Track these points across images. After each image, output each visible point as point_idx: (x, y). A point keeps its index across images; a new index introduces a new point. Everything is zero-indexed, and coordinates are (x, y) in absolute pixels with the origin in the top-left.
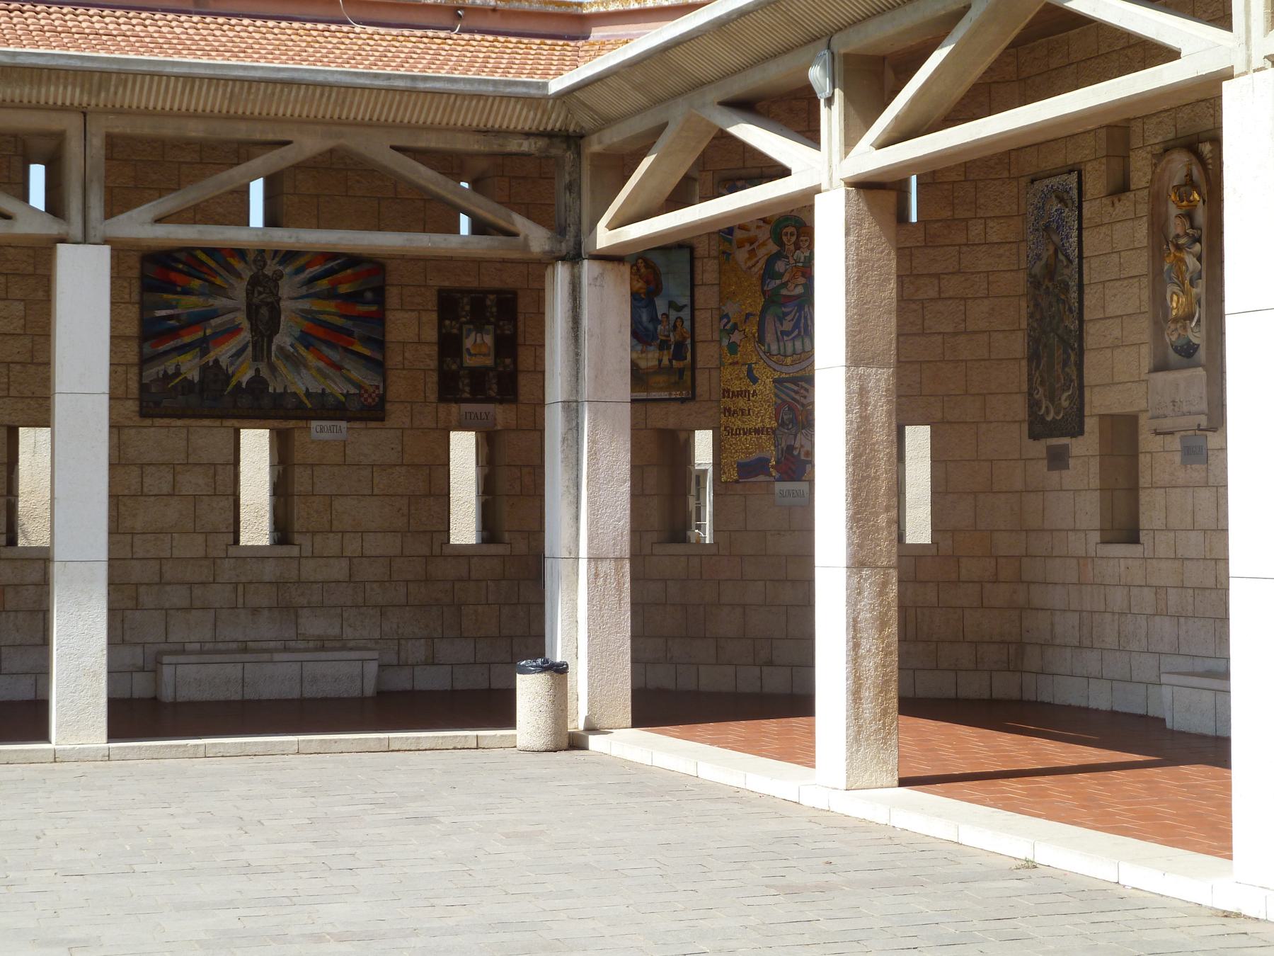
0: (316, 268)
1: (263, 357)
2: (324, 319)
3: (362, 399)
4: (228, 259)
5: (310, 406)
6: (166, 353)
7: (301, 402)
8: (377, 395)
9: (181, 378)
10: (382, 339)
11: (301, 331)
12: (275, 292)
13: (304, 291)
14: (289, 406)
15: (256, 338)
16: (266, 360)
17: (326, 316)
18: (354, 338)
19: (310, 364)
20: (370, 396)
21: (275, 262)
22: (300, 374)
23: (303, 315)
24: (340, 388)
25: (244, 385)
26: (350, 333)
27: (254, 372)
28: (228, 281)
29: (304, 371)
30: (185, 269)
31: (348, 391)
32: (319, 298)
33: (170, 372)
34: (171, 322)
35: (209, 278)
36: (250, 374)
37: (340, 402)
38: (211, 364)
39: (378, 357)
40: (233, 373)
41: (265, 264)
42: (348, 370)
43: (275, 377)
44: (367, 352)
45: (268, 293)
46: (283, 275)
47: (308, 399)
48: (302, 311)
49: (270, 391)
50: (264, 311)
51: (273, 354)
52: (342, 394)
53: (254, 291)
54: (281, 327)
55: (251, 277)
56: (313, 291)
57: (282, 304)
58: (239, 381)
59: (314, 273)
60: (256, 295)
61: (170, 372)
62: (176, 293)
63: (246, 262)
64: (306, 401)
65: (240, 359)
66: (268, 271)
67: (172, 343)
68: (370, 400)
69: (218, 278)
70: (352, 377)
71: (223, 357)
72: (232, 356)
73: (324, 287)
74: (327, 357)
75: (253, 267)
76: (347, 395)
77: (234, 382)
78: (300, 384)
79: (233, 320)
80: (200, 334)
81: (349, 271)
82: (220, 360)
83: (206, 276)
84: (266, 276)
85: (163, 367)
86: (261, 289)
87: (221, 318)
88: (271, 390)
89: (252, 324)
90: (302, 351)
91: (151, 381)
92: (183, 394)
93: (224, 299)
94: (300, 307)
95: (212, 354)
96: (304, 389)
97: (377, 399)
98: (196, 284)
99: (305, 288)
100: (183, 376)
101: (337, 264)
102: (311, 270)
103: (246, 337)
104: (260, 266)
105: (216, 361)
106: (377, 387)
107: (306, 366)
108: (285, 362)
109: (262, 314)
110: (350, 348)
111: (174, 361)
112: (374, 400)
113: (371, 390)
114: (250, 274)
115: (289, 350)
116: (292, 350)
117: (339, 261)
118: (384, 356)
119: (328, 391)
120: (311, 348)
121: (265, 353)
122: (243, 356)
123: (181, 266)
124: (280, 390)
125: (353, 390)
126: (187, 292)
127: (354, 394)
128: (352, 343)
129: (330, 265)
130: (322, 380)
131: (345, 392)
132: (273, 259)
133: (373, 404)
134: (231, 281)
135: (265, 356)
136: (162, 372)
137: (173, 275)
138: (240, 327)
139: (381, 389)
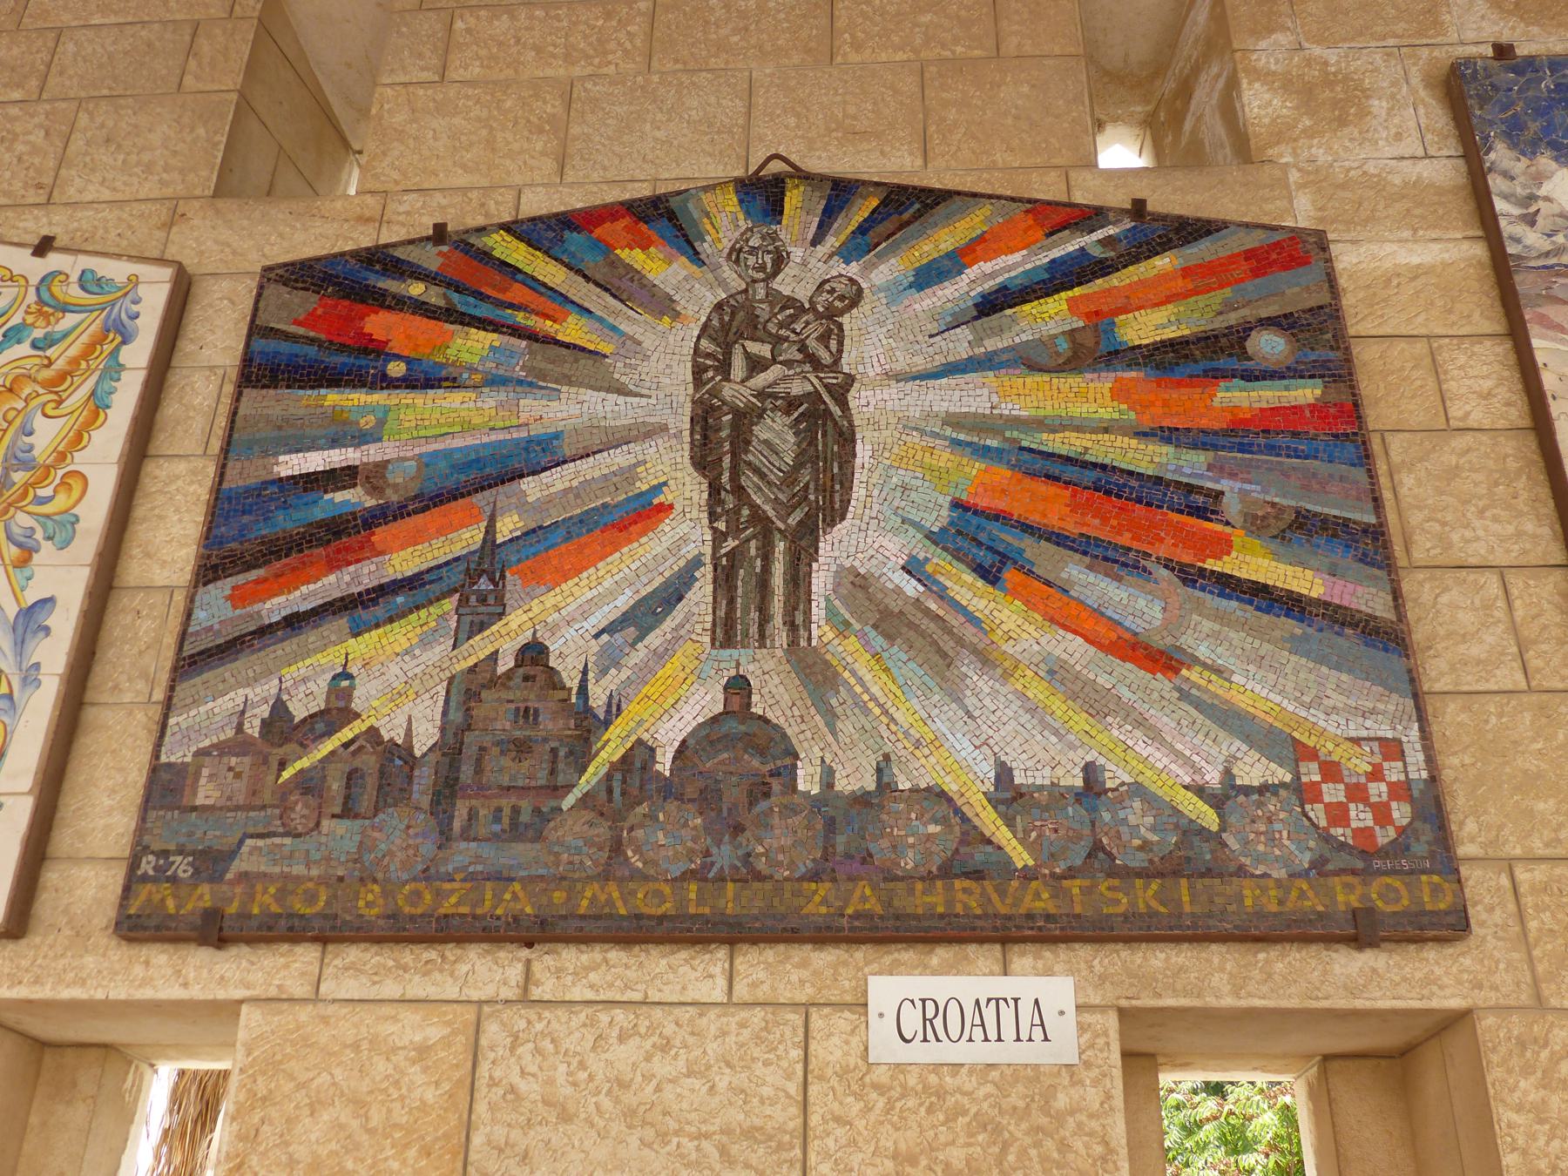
0: (1017, 257)
1: (765, 619)
2: (1063, 450)
3: (1317, 813)
4: (623, 254)
5: (1021, 857)
6: (294, 622)
7: (974, 836)
8: (1400, 791)
9: (346, 734)
10: (1373, 520)
11: (957, 504)
12: (826, 358)
13: (961, 344)
14: (909, 862)
15: (731, 543)
16: (781, 638)
17: (1072, 436)
18: (1228, 523)
19: (1007, 647)
20: (1357, 793)
21: (822, 250)
22: (959, 701)
23: (962, 437)
24: (1188, 762)
25: (664, 763)
26: (1202, 504)
27: (721, 697)
28: (614, 328)
29: (979, 681)
30: (435, 296)
31: (1228, 773)
32: (1034, 367)
33: (299, 711)
34: (339, 497)
35: (532, 322)
36: (705, 702)
37: (1192, 831)
38: (506, 664)
39: (1369, 599)
40: (614, 708)
41: (780, 261)
42: (1218, 671)
43: (831, 717)
44: (1306, 582)
45: (788, 364)
46: (860, 291)
47: (1010, 824)
48: (953, 421)
49: (802, 786)
50: (776, 432)
51: (818, 612)
52: (1200, 791)
53: (728, 354)
54: (858, 492)
55: (719, 307)
56: (992, 344)
57: (858, 399)
58: (640, 742)
59: (1000, 279)
60: (738, 367)
61: (299, 711)
62: (388, 383)
63: (696, 257)
64: (1003, 835)
65: (654, 639)
66: (795, 283)
67: (332, 578)
68: (1361, 817)
69: (572, 319)
70: (1243, 702)
71: (570, 633)
72: (610, 629)
73: (1053, 328)
74: (1097, 613)
75: (728, 272)
76: (1223, 797)
77: (612, 746)
78: (963, 746)
79: (629, 474)
80: (470, 538)
81: (1163, 263)
82: (553, 647)
83: (520, 318)
84: (790, 302)
85: (272, 687)
86: (763, 350)
87: (570, 467)
88: (807, 780)
89: (715, 490)
90: (965, 587)
91: (202, 753)
92: (347, 812)
93: (589, 395)
94: (942, 407)
95: (515, 619)
96: (988, 770)
97: (1401, 813)
98: (471, 346)
99: (964, 333)
100: (357, 727)
101: (1107, 242)
102: (987, 267)
103: (684, 539)
104: (762, 268)
105: (533, 653)
106: (1392, 749)
107: (986, 659)
108: (879, 642)
109: (766, 442)
110: (1211, 564)
111: (330, 659)
112: (1382, 814)
113: (1358, 764)
114: (710, 298)
115: (898, 591)
116: (911, 587)
117: (1111, 230)
118: (1396, 595)
119: (1116, 775)
120: (1009, 575)
121: (777, 606)
122: (669, 624)
123: (416, 289)
124: (855, 778)
125: (1254, 770)
126: (424, 379)
127: (1264, 789)
128: (1223, 546)
129: (1071, 248)
130: (1081, 721)
131: (1213, 777)
132: (814, 243)
133: (1385, 836)
134: (624, 327)
135: (778, 620)
136: (264, 711)
137: (378, 324)
138: (661, 498)
139: (1416, 757)
